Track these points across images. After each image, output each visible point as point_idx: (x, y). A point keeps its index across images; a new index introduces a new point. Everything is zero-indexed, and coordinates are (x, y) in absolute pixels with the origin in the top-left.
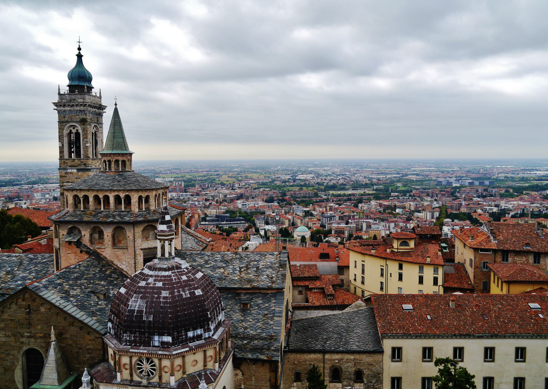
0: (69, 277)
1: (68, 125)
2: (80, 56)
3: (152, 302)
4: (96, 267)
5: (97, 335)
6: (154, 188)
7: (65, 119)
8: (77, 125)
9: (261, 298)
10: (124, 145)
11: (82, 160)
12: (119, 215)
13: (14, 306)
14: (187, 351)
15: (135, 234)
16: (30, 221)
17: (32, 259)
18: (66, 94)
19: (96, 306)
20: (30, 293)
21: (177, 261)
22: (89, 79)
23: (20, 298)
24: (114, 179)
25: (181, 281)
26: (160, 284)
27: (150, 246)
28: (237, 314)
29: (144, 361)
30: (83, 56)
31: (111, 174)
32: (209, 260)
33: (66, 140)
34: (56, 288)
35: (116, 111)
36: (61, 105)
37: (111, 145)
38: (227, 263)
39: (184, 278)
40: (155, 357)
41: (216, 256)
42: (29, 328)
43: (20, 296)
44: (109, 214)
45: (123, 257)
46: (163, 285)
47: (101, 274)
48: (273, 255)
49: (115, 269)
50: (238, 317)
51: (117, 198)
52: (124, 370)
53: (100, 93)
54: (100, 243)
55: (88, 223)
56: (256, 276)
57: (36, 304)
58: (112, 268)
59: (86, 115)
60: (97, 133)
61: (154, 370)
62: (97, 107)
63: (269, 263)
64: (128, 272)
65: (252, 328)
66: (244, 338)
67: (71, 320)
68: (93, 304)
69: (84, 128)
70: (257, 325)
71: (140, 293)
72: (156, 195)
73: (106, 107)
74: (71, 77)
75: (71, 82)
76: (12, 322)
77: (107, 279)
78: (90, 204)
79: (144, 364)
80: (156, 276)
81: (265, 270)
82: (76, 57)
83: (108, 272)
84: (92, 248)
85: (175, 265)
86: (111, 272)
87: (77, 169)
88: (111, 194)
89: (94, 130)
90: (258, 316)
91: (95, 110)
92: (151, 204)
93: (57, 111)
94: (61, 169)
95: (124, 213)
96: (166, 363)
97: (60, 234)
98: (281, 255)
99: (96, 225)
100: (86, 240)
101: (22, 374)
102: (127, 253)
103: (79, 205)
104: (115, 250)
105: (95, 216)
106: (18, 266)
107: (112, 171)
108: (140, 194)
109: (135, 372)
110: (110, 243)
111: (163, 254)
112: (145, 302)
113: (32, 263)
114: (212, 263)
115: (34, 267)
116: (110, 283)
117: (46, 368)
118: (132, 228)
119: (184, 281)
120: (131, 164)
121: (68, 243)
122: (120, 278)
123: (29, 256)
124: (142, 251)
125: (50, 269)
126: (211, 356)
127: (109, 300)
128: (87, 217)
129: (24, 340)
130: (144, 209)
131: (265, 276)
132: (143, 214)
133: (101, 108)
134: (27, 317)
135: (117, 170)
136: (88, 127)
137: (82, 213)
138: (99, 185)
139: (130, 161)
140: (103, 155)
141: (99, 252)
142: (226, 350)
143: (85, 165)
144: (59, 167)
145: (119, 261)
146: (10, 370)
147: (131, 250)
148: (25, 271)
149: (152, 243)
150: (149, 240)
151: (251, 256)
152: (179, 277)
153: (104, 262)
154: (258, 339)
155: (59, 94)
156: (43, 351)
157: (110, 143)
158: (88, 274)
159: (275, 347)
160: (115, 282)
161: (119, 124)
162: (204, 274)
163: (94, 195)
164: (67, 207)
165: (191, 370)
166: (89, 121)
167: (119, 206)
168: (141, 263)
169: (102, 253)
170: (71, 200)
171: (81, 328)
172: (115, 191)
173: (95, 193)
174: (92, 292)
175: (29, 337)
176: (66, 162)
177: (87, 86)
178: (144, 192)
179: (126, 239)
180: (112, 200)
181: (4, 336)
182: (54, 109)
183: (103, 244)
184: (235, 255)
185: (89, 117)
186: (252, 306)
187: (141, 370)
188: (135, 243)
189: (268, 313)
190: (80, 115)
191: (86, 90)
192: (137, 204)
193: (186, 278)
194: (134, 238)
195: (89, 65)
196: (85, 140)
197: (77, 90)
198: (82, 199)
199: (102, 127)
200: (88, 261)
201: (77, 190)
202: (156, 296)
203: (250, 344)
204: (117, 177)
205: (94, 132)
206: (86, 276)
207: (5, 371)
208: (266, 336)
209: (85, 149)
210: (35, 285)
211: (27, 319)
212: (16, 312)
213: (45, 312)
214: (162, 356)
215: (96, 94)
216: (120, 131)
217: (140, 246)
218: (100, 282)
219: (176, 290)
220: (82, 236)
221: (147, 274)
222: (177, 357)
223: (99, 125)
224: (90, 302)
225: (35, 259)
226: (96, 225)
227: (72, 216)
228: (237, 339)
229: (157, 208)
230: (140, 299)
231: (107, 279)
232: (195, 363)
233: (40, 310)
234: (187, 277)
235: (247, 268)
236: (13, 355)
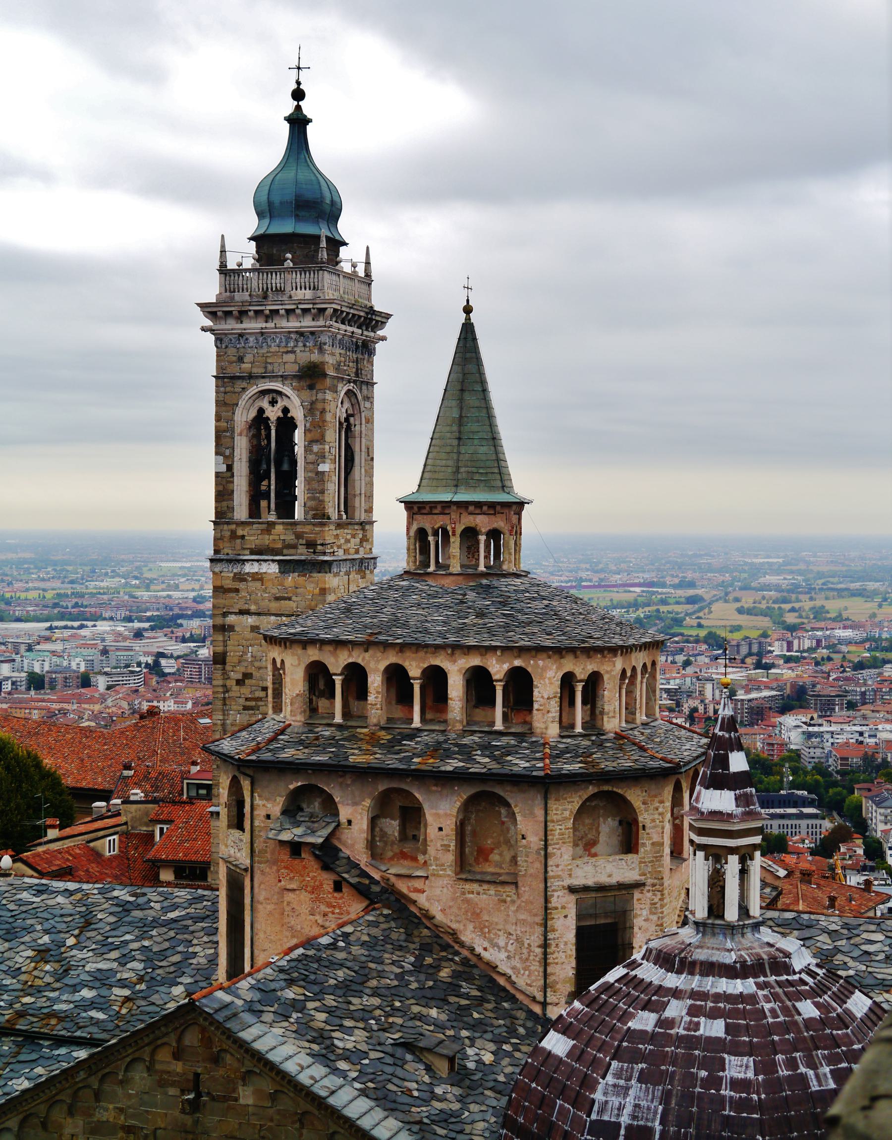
0: (320, 978)
1: (253, 390)
3: (688, 1097)
4: (401, 948)
6: (621, 643)
7: (243, 366)
8: (287, 390)
11: (299, 529)
12: (486, 748)
13: (140, 1077)
15: (550, 826)
16: (38, 765)
17: (125, 908)
18: (246, 270)
19: (426, 1102)
20: (203, 1030)
21: (772, 942)
23: (165, 1044)
24: (462, 602)
25: (795, 1023)
26: (715, 1028)
27: (604, 879)
30: (310, 121)
31: (448, 583)
32: (837, 950)
33: (242, 446)
34: (286, 1018)
35: (470, 336)
36: (228, 314)
37: (450, 470)
39: (808, 1009)
41: (865, 936)
43: (165, 1040)
44: (446, 741)
45: (497, 918)
46: (727, 1032)
47: (422, 977)
49: (465, 962)
53: (368, 263)
54: (403, 856)
55: (364, 774)
57: (222, 1072)
58: (457, 958)
59: (321, 350)
60: (352, 419)
62: (360, 317)
64: (514, 978)
68: (416, 1094)
69: (313, 403)
71: (634, 1057)
72: (624, 671)
73: (388, 316)
75: (266, 221)
77: (445, 1001)
78: (371, 698)
80: (694, 995)
82: (287, 126)
83: (444, 974)
84: (376, 876)
85: (765, 957)
86: (456, 975)
87: (279, 561)
88: (455, 661)
89: (344, 410)
91: (350, 329)
92: (606, 708)
93: (213, 337)
94: (220, 560)
95: (505, 740)
99: (395, 785)
102: (513, 902)
104: (468, 886)
105: (391, 747)
106: (76, 932)
108: (569, 665)
110: (450, 858)
112: (658, 1094)
113: (130, 923)
114: (851, 963)
115: (138, 939)
116: (460, 1015)
118: (539, 801)
119: (809, 1023)
120: (517, 545)
121: (287, 850)
122: (488, 1002)
123: (116, 893)
124: (573, 898)
125: (197, 949)
127: (467, 1082)
128: (359, 749)
130: (579, 729)
132: (578, 746)
134: (188, 1120)
135: (468, 567)
136: (329, 396)
137: (338, 735)
139: (517, 531)
141: (405, 890)
143: (311, 545)
144: (210, 552)
145: (481, 930)
147: (531, 890)
148: (104, 949)
149: (610, 868)
150: (595, 855)
152: (789, 1003)
153: (426, 932)
155: (223, 270)
158: (381, 975)
160: (476, 1015)
161: (478, 388)
162: (874, 1002)
164: (278, 709)
166: (331, 372)
168: (566, 944)
169: (413, 896)
173: (392, 658)
174: (408, 1046)
176: (240, 532)
178: (583, 658)
180: (456, 687)
182: (204, 329)
183: (415, 859)
185: (331, 358)
188: (550, 862)
190: (298, 350)
191: (324, 255)
192: (554, 706)
193: (815, 1013)
194: (546, 840)
196: (316, 448)
197: (289, 256)
198: (338, 680)
199: (369, 398)
200: (370, 924)
201: (323, 643)
202: (703, 1074)
204: (471, 596)
206: (374, 983)
209: (315, 485)
210: (220, 1001)
211: (187, 1132)
212: (146, 1097)
213: (255, 1106)
215: (354, 266)
216: (484, 413)
217: (565, 875)
218: (424, 1011)
219: (780, 1057)
220: (339, 825)
221: (656, 982)
223: (361, 390)
224: (407, 1084)
225: (140, 907)
226: (395, 785)
227: (301, 742)
229: (624, 724)
230: (640, 1080)
231: (445, 1001)
233: (236, 1099)
234: (817, 1005)
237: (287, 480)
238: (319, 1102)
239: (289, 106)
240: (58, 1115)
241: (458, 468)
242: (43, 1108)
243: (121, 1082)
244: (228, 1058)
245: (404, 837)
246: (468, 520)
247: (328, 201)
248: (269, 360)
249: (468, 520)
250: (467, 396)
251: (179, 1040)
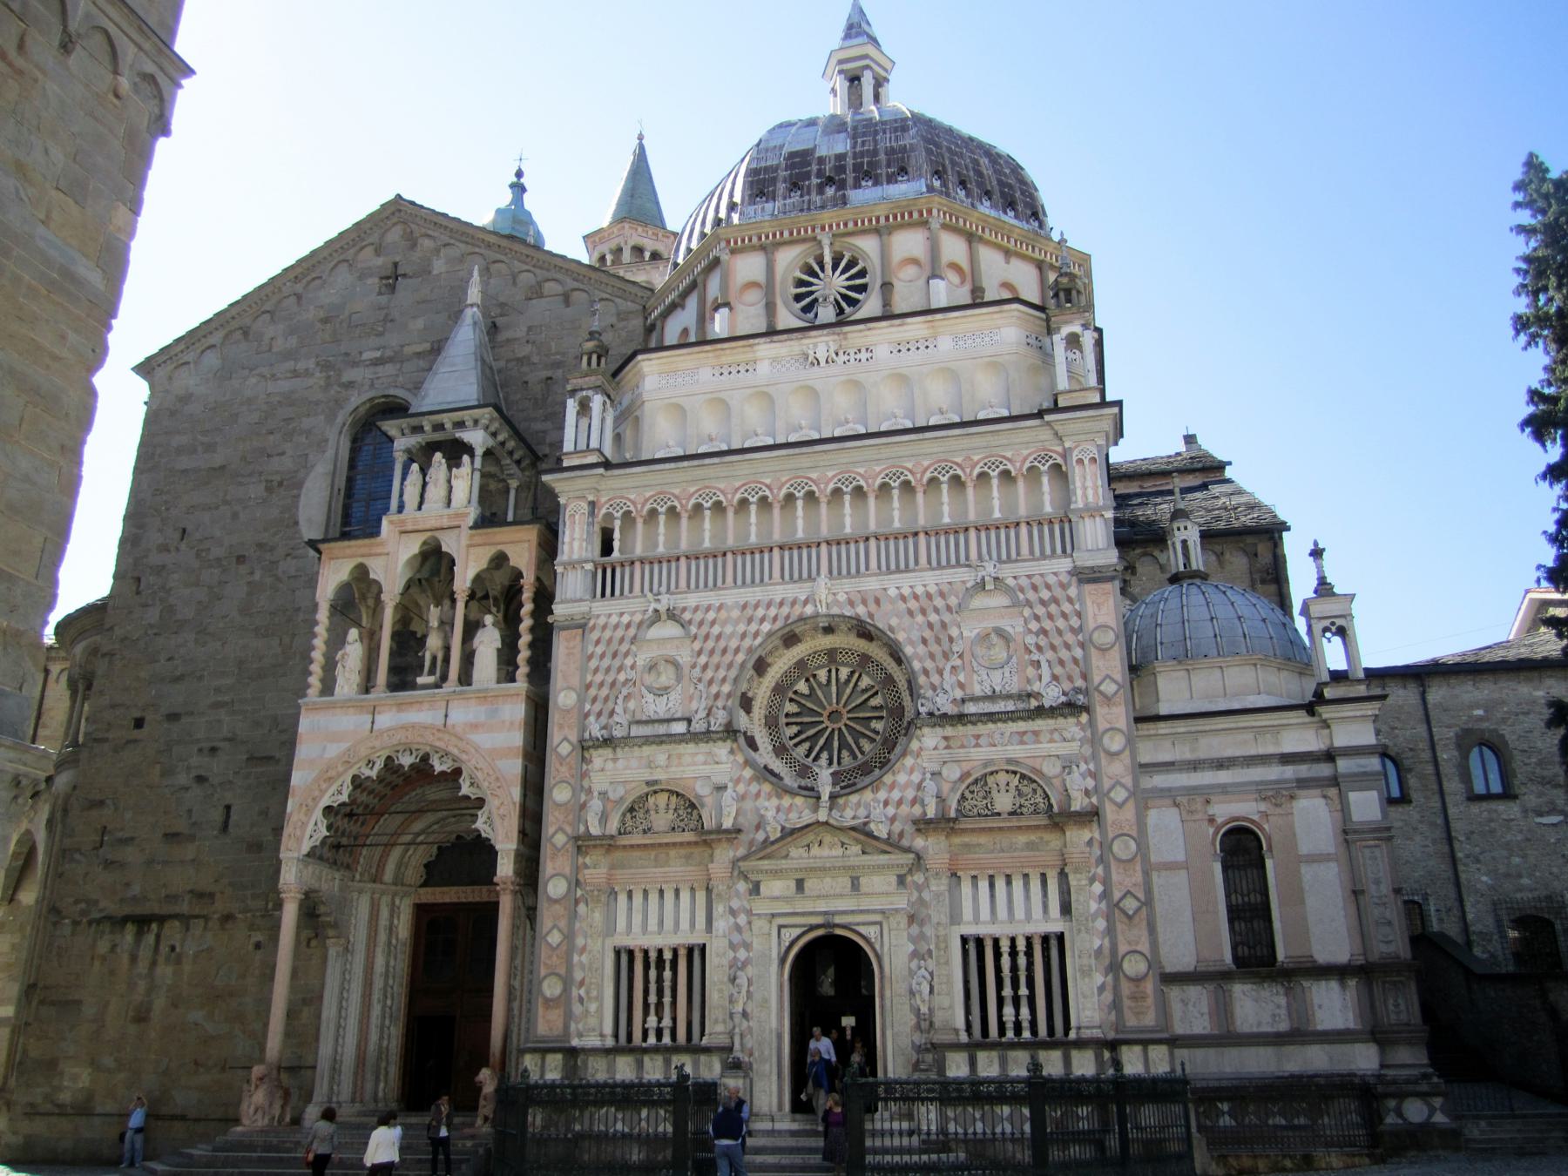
82: (509, 191)
207: (269, 489)
236: (308, 433)
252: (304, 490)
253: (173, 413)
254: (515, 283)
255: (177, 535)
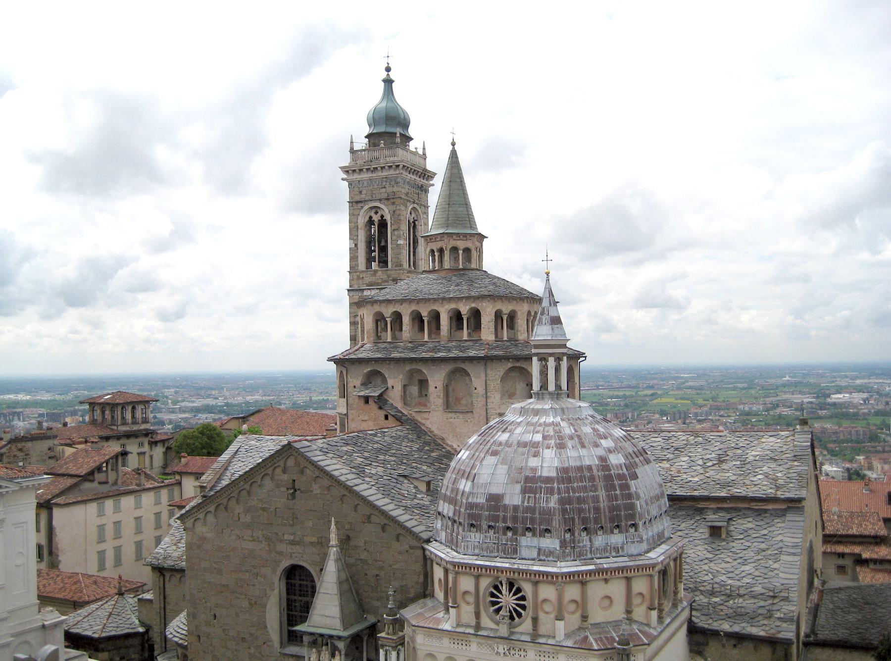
1: (366, 207)
2: (388, 82)
4: (413, 441)
5: (414, 543)
8: (382, 206)
9: (750, 519)
10: (467, 218)
13: (267, 482)
14: (590, 572)
15: (488, 382)
19: (412, 500)
22: (404, 123)
23: (278, 466)
26: (538, 437)
28: (698, 548)
29: (502, 586)
33: (362, 235)
37: (444, 219)
38: (676, 452)
40: (526, 580)
42: (292, 526)
47: (422, 454)
48: (778, 437)
49: (448, 452)
50: (699, 553)
51: (457, 317)
52: (463, 605)
53: (424, 149)
54: (420, 404)
56: (740, 475)
60: (416, 222)
61: (524, 607)
63: (768, 452)
65: (730, 575)
66: (712, 593)
67: (367, 510)
68: (406, 495)
69: (394, 212)
70: (742, 569)
74: (373, 120)
76: (265, 513)
78: (404, 328)
79: (504, 592)
81: (760, 464)
88: (443, 307)
90: (744, 552)
92: (520, 329)
93: (347, 183)
95: (468, 343)
96: (547, 592)
97: (348, 385)
98: (796, 436)
100: (395, 397)
101: (278, 614)
103: (383, 335)
104: (450, 415)
105: (412, 350)
107: (446, 267)
108: (499, 306)
109: (484, 609)
110: (440, 401)
111: (544, 386)
117: (320, 595)
118: (482, 368)
121: (362, 401)
126: (641, 594)
128: (398, 351)
129: (281, 547)
130: (505, 338)
131: (760, 477)
133: (427, 175)
136: (403, 208)
138: (421, 292)
140: (429, 239)
141: (420, 420)
142: (675, 600)
144: (348, 287)
145: (456, 437)
146: (258, 604)
151: (728, 439)
154: (744, 595)
155: (352, 151)
156: (316, 571)
157: (442, 216)
159: (784, 614)
161: (458, 180)
163: (411, 310)
165: (597, 615)
167: (458, 333)
169: (423, 422)
170: (369, 323)
171: (384, 528)
172: (451, 299)
173: (414, 307)
174: (405, 476)
175: (292, 543)
177: (400, 134)
179: (471, 396)
181: (251, 539)
182: (343, 179)
183: (425, 405)
184: (693, 437)
185: (402, 190)
186: (730, 533)
187: (496, 607)
188: (488, 401)
189: (767, 547)
191: (398, 140)
194: (486, 390)
195: (404, 98)
196: (396, 233)
197: (382, 142)
198: (389, 320)
203: (726, 604)
204: (454, 278)
205: (412, 220)
206: (394, 451)
208: (763, 591)
213: (320, 494)
214: (539, 576)
216: (461, 192)
218: (419, 466)
222: (571, 582)
228: (698, 593)
232: (607, 602)
235: (720, 461)
237: (383, 249)
238: (350, 489)
239: (384, 74)
240: (232, 503)
241: (448, 218)
242: (225, 501)
243: (260, 486)
244: (308, 472)
245: (421, 395)
246: (453, 243)
247: (402, 117)
248: (374, 192)
249: (453, 243)
250: (452, 184)
251: (285, 464)
252: (267, 610)
253: (199, 547)
254: (356, 511)
255: (212, 618)
